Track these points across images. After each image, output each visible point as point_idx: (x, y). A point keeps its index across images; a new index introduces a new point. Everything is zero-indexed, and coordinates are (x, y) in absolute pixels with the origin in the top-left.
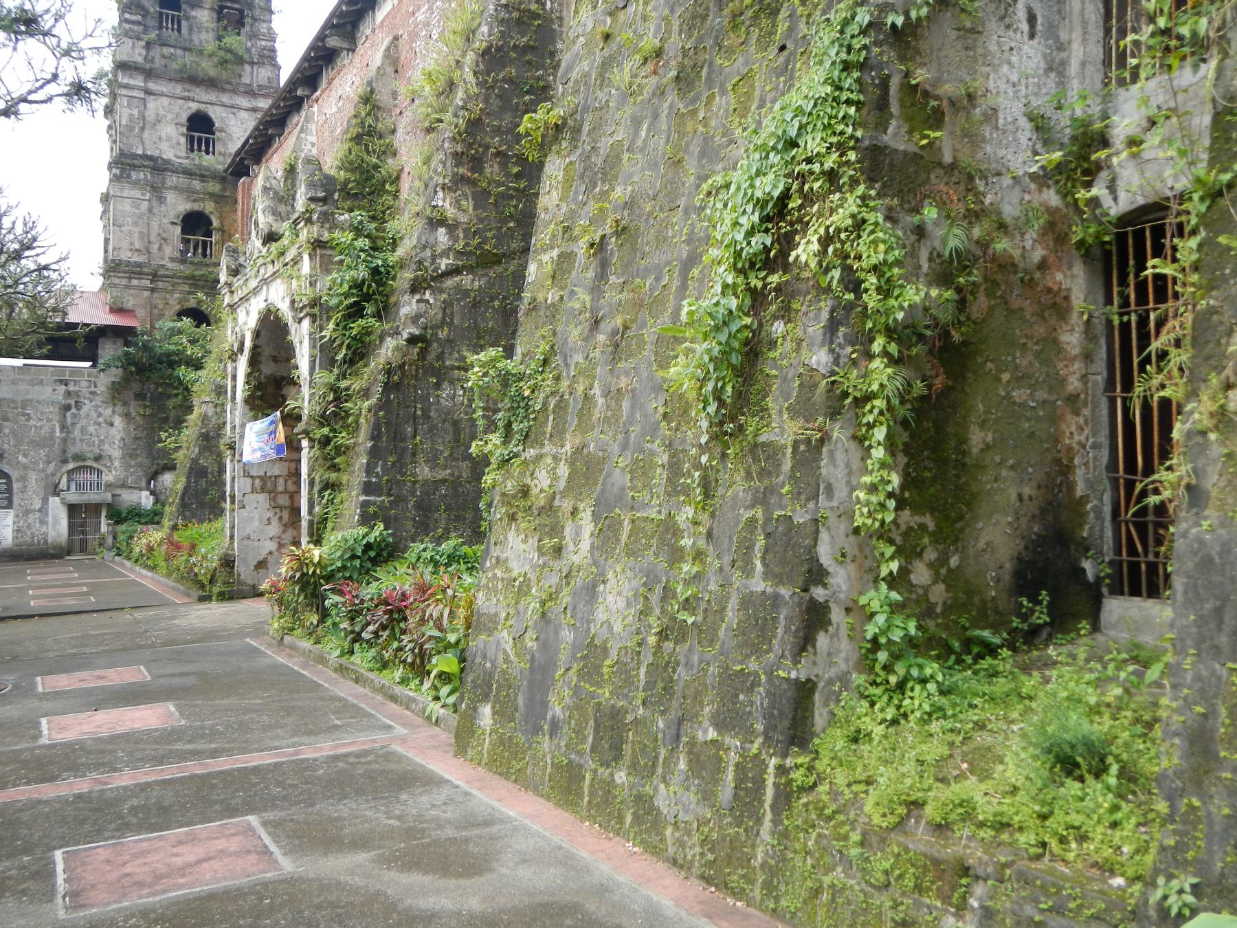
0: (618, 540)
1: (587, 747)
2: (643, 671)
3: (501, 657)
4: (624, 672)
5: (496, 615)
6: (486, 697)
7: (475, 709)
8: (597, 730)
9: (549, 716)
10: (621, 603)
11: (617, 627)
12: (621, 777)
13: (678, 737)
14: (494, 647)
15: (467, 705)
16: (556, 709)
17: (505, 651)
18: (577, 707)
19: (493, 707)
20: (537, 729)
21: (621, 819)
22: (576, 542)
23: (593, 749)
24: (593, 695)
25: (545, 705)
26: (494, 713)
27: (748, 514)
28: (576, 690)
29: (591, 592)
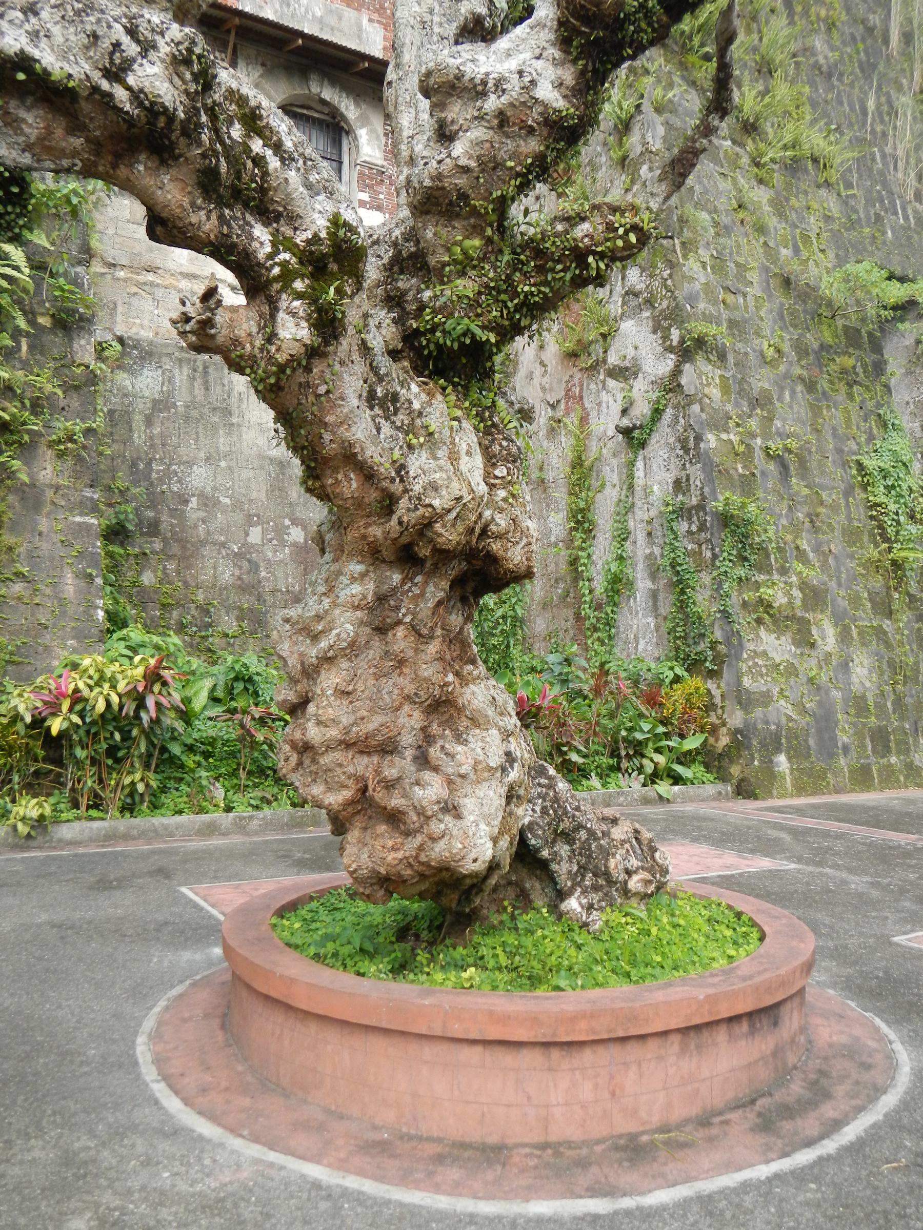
0: (852, 637)
1: (870, 752)
2: (889, 704)
3: (784, 720)
4: (880, 707)
5: (768, 691)
6: (778, 750)
7: (771, 761)
8: (872, 742)
9: (840, 744)
10: (866, 672)
11: (868, 684)
12: (893, 760)
13: (916, 730)
14: (775, 714)
15: (760, 761)
16: (844, 738)
17: (786, 714)
18: (856, 734)
19: (788, 753)
20: (832, 755)
21: (898, 781)
22: (823, 639)
23: (874, 751)
24: (864, 725)
25: (834, 739)
26: (789, 759)
27: (917, 626)
28: (853, 724)
29: (845, 666)
